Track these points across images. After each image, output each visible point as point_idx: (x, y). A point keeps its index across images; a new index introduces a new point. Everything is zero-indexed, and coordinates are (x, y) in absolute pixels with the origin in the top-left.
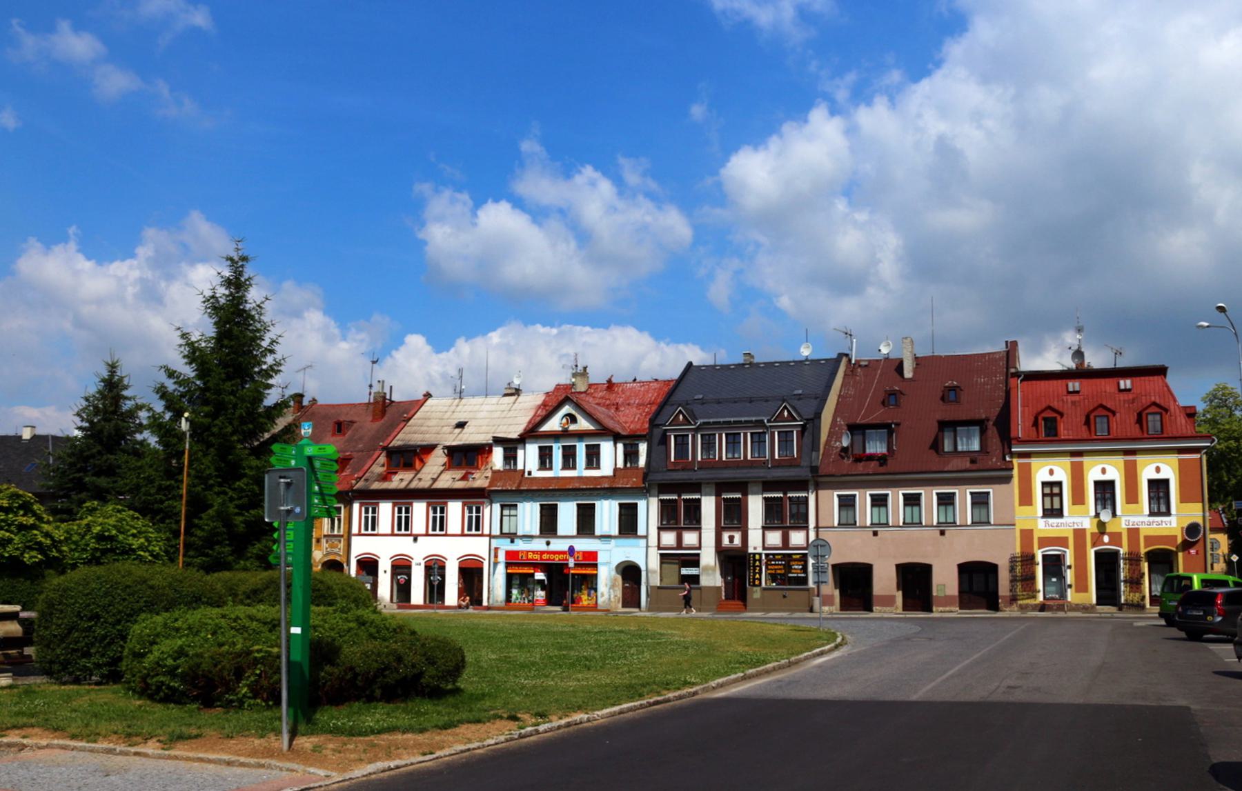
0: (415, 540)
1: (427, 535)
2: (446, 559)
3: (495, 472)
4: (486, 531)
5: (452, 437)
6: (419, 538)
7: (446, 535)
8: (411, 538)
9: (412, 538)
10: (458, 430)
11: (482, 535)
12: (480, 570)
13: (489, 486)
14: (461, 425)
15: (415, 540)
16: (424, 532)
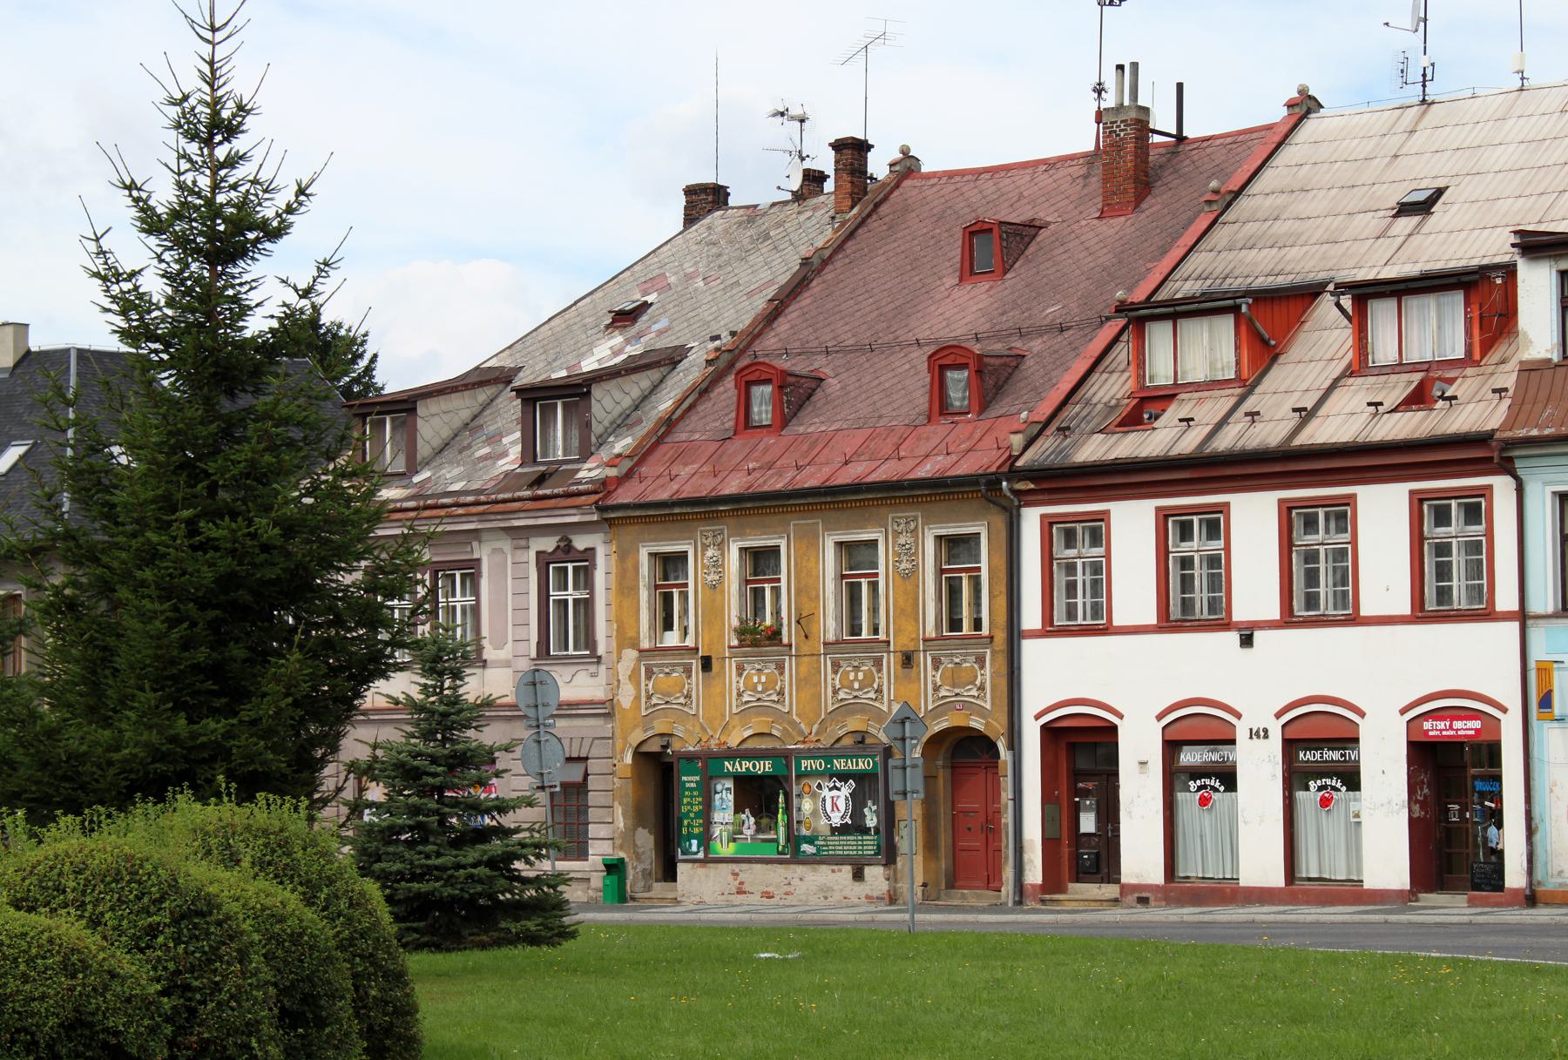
0: (1247, 641)
1: (1288, 620)
2: (1362, 714)
3: (1530, 370)
4: (1506, 599)
5: (1386, 247)
6: (1259, 636)
7: (1355, 620)
8: (1233, 637)
9: (1233, 637)
10: (1407, 223)
11: (1488, 614)
12: (1491, 753)
13: (1512, 420)
14: (1421, 208)
15: (1247, 641)
16: (1274, 613)
